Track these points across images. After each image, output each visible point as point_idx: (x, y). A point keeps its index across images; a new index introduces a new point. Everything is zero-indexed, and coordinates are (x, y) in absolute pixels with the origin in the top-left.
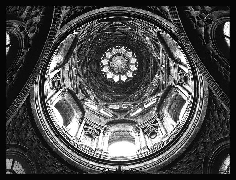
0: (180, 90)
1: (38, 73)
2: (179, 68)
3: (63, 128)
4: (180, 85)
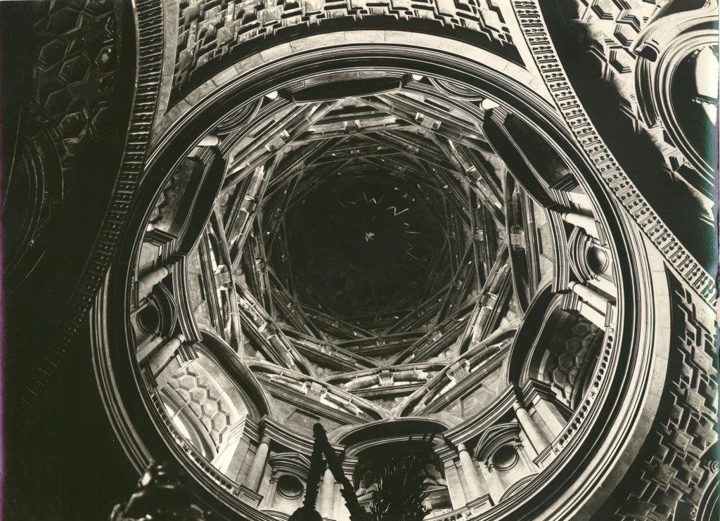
0: (580, 299)
2: (569, 227)
4: (577, 282)
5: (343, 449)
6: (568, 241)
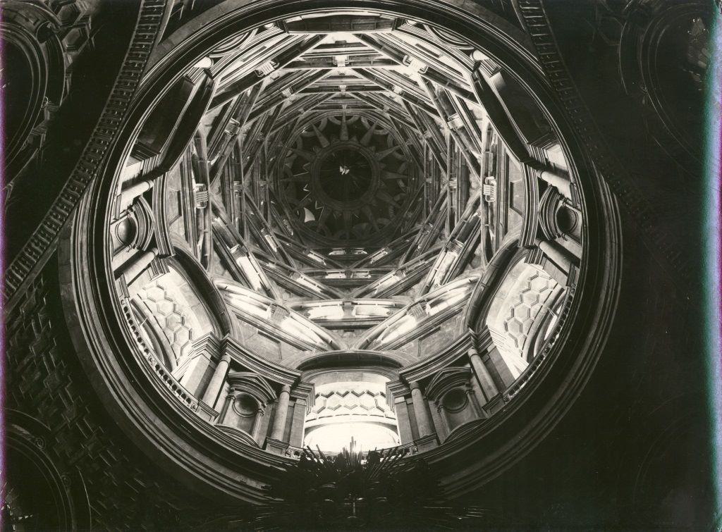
0: (545, 255)
1: (88, 184)
2: (543, 185)
3: (162, 372)
5: (299, 375)
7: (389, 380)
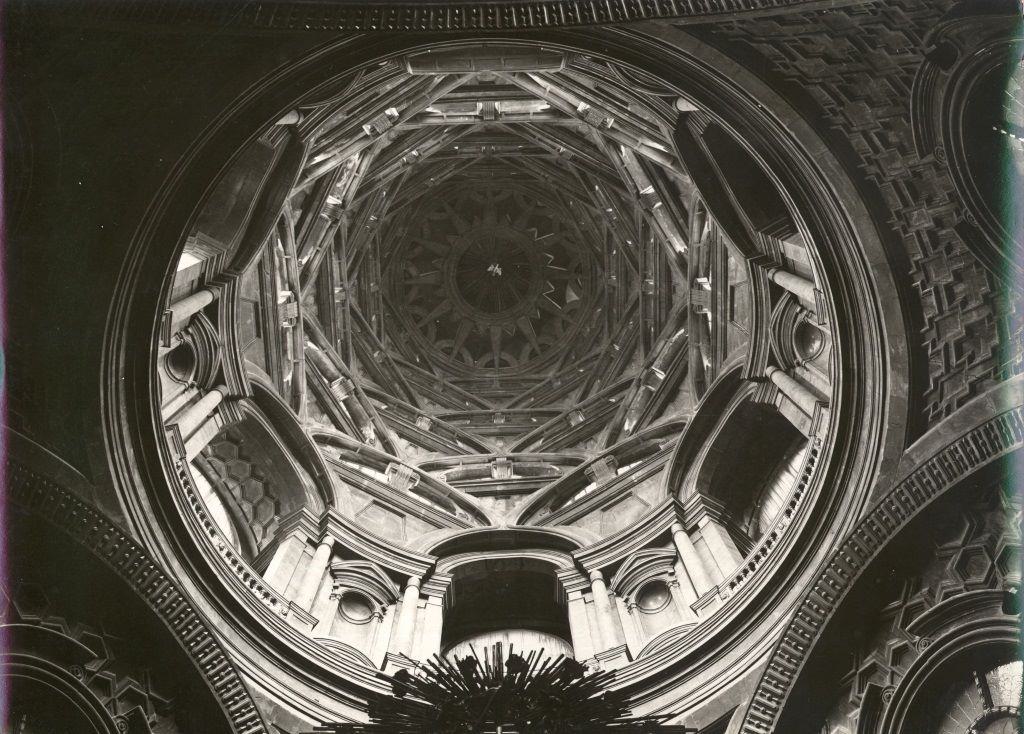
0: (780, 391)
2: (777, 291)
6: (772, 310)
7: (438, 654)
